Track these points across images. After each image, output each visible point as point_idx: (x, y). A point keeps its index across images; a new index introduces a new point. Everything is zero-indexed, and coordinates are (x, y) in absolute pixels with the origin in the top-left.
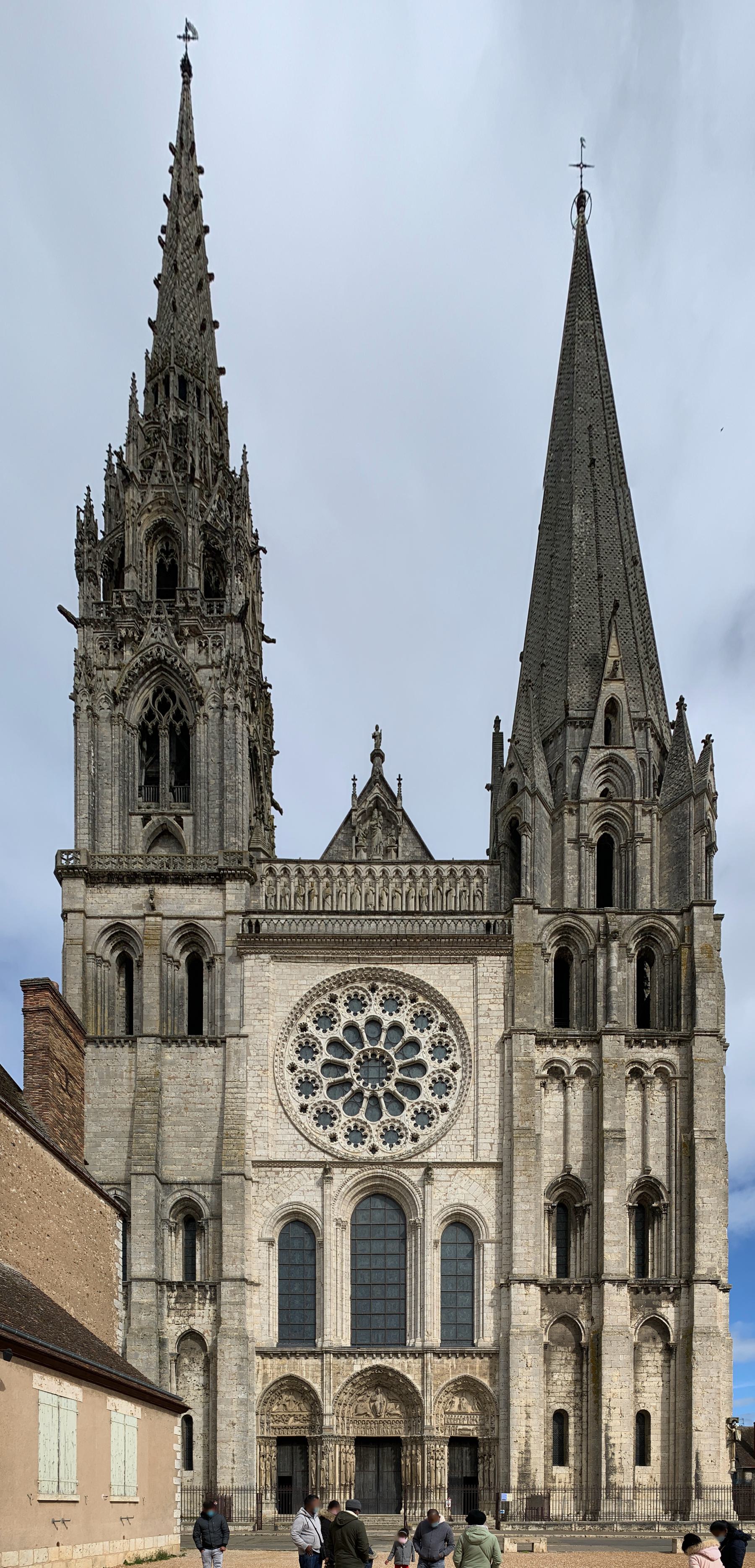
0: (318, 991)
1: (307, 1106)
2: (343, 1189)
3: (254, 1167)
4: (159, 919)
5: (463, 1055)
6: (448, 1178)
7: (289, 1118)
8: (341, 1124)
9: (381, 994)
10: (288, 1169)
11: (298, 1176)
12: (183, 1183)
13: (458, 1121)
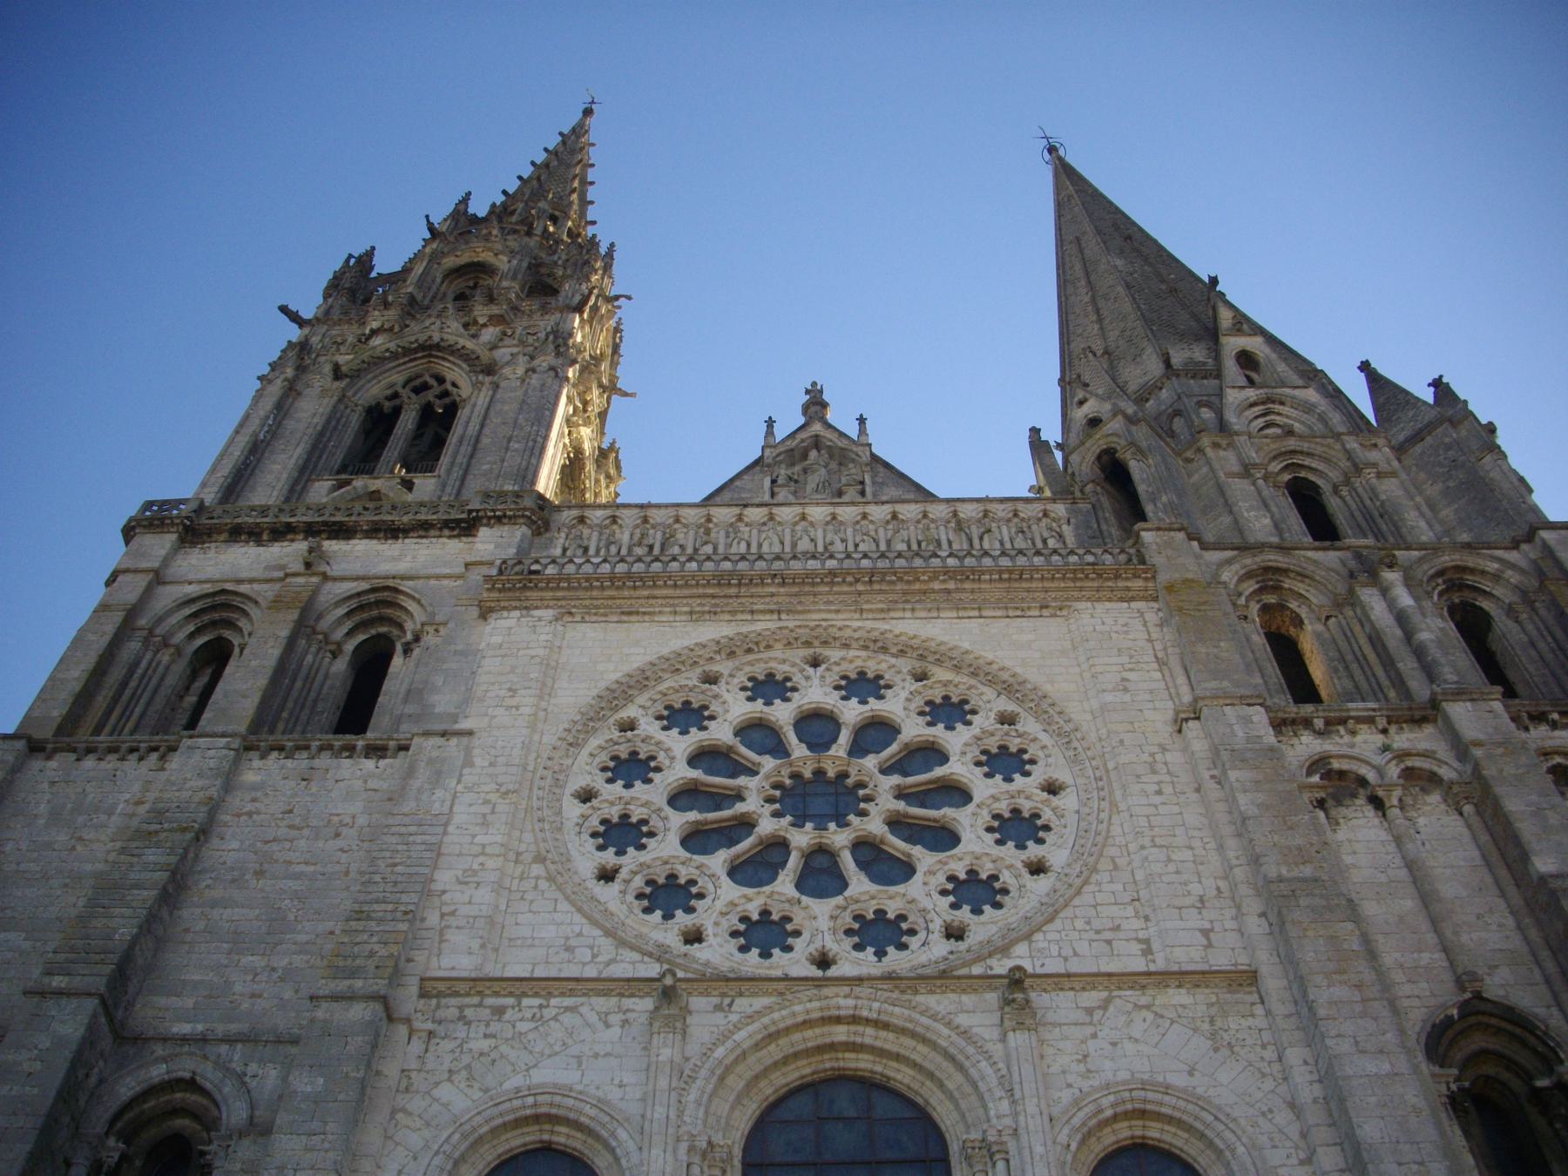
0: (674, 663)
2: (720, 1052)
3: (423, 995)
4: (314, 580)
6: (1080, 1016)
7: (559, 889)
8: (720, 905)
9: (836, 669)
10: (536, 1002)
11: (567, 1018)
12: (185, 1039)
13: (1085, 889)
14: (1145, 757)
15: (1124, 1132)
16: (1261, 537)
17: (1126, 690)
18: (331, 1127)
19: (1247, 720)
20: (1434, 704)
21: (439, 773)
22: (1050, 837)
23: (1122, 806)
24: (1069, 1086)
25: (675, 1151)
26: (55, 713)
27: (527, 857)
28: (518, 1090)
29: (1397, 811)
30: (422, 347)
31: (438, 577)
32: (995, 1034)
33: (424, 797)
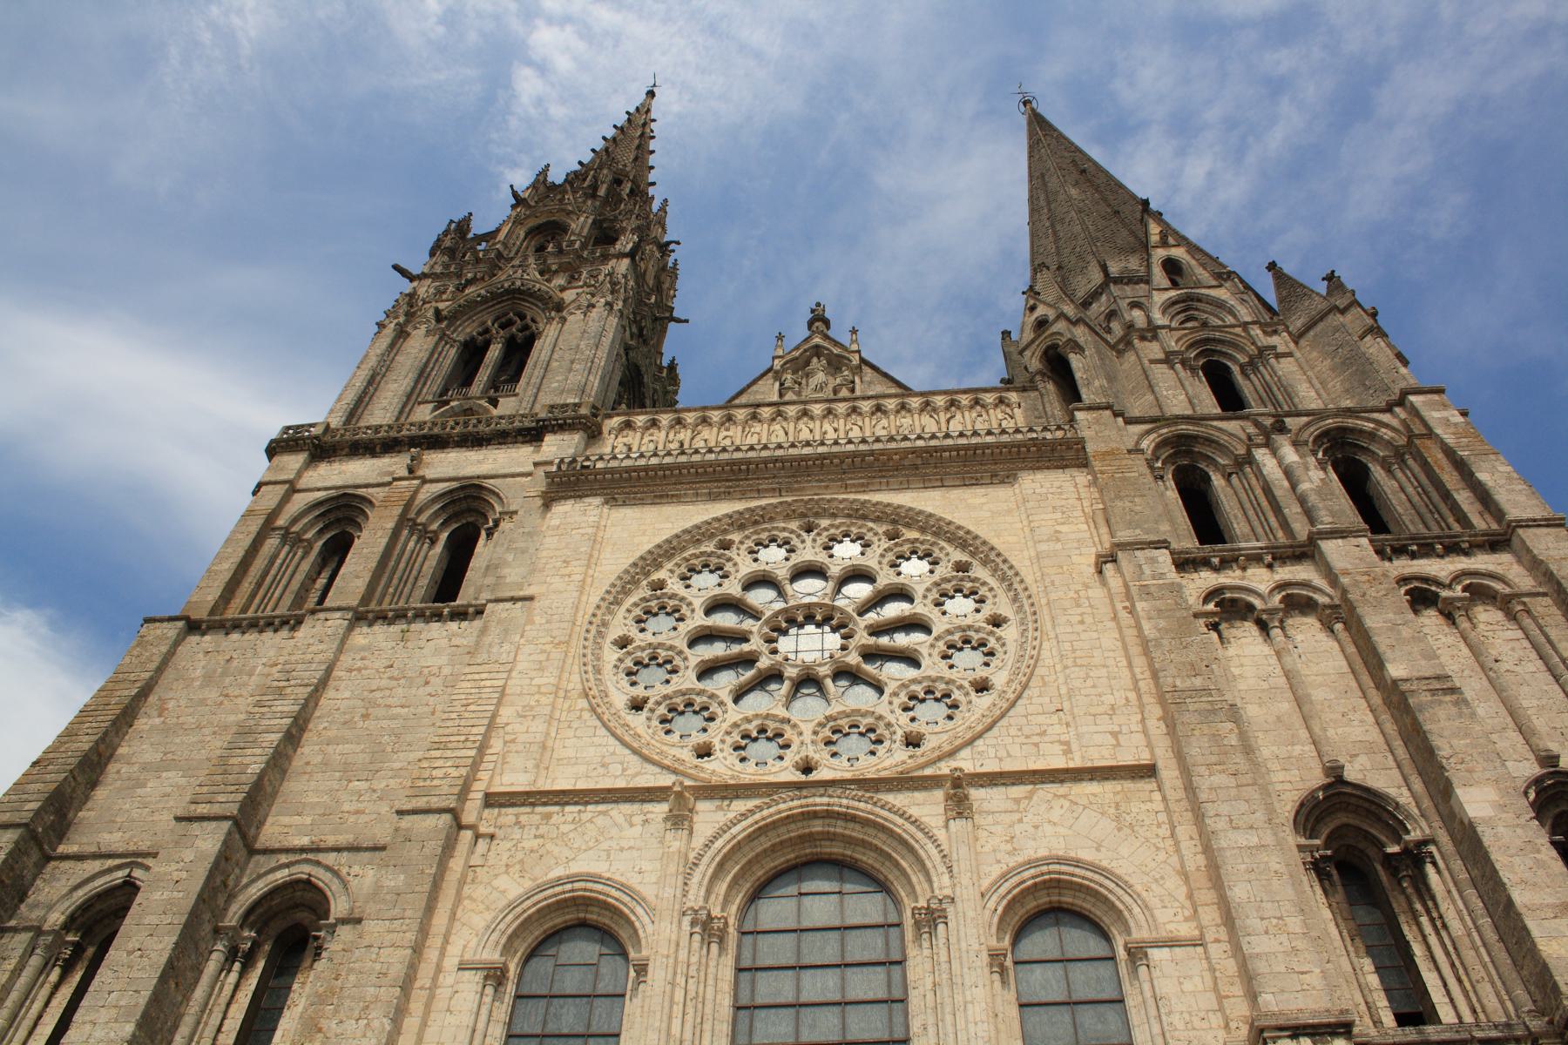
0: (696, 535)
1: (645, 700)
2: (719, 843)
4: (416, 482)
5: (1015, 599)
6: (1010, 805)
7: (599, 718)
8: (725, 726)
11: (600, 821)
14: (1072, 594)
15: (1043, 900)
16: (1177, 411)
17: (1058, 540)
18: (409, 913)
19: (1153, 561)
20: (1312, 540)
21: (506, 631)
22: (995, 662)
23: (1052, 635)
24: (999, 862)
25: (680, 922)
26: (210, 598)
27: (574, 694)
28: (560, 879)
29: (1278, 631)
30: (508, 291)
31: (513, 476)
32: (941, 821)
33: (494, 650)
